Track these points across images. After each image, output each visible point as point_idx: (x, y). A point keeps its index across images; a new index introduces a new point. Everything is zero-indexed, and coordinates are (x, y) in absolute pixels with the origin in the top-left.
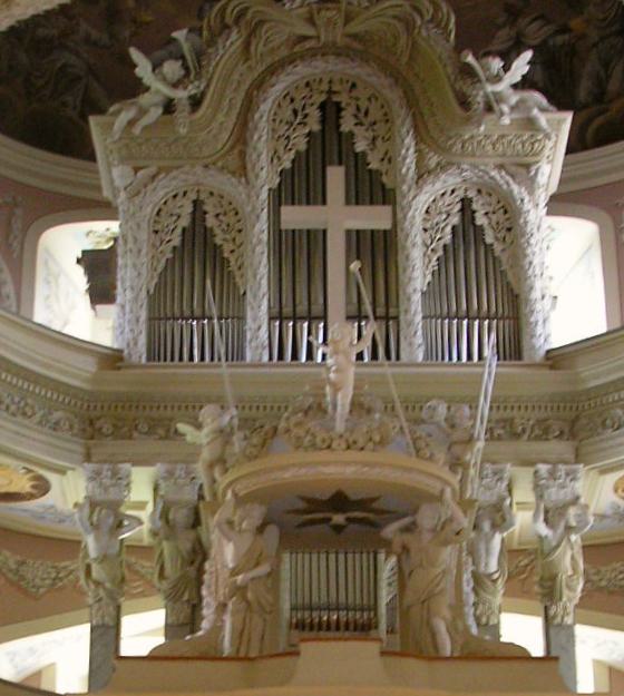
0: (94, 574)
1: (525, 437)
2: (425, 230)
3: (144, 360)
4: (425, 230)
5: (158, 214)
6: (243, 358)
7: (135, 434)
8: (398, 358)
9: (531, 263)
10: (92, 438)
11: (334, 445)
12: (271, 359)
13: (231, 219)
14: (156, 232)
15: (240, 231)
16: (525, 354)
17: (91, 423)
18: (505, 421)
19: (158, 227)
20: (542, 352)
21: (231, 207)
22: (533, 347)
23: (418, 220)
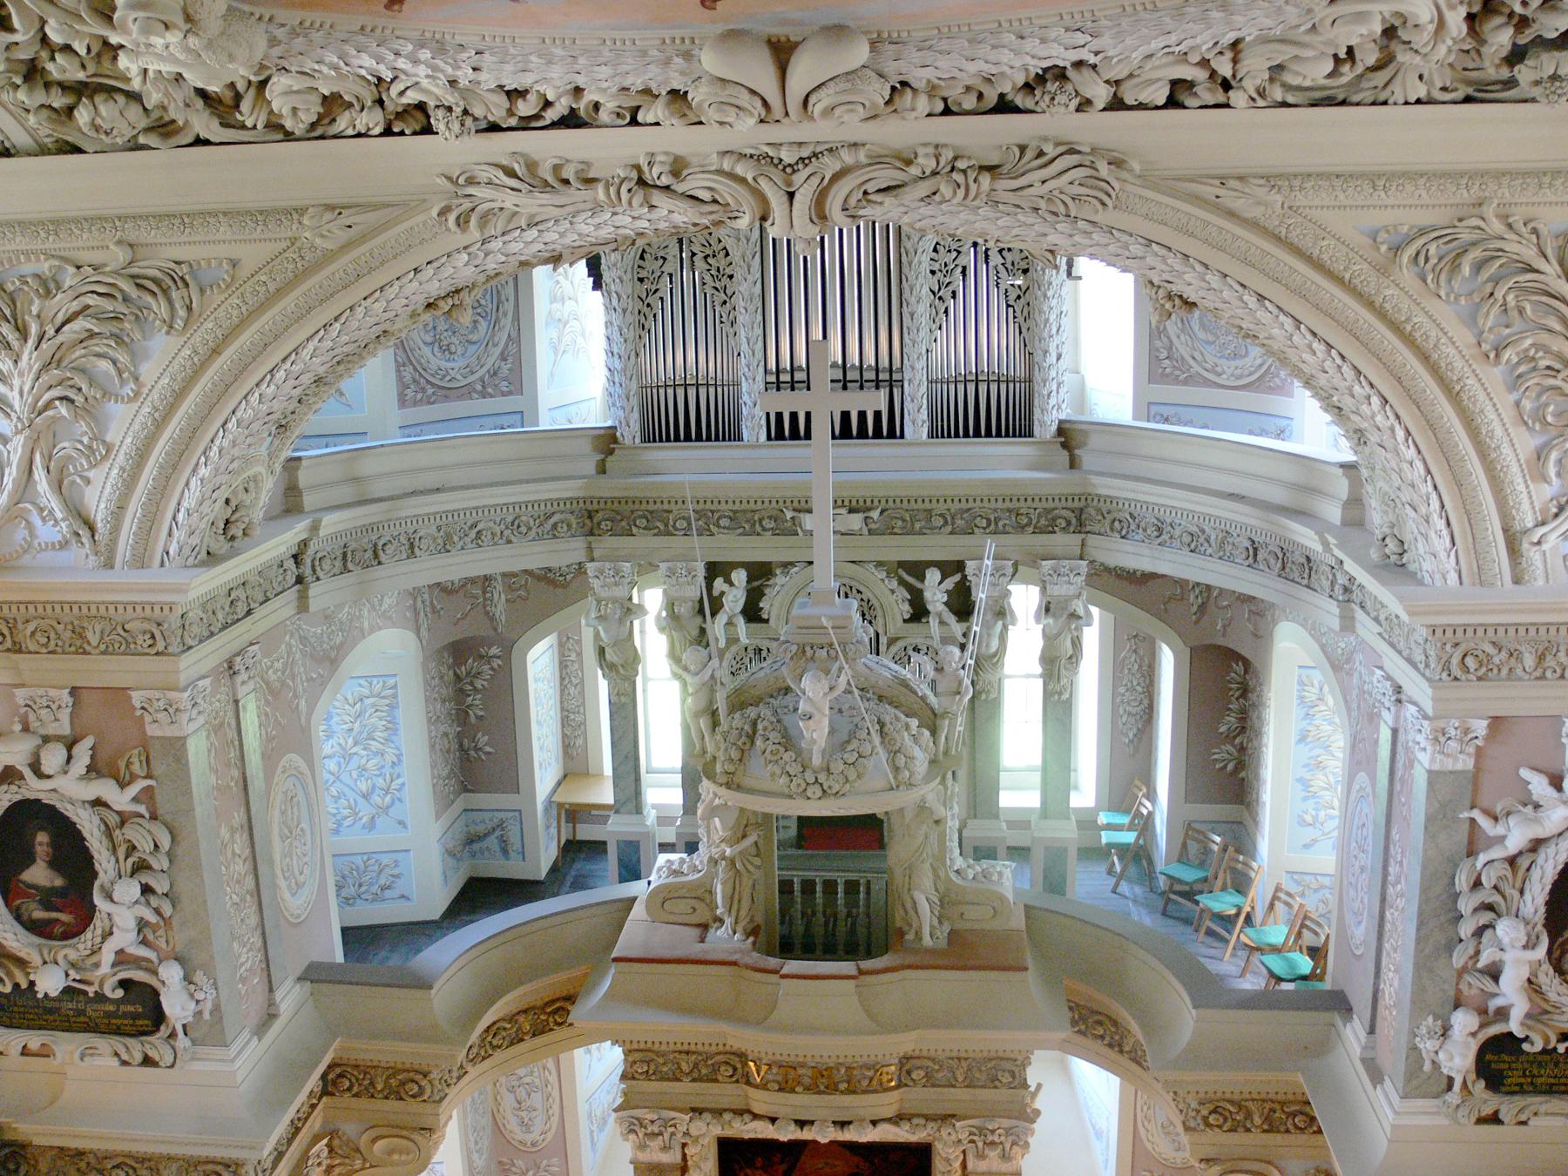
0: (607, 656)
1: (1031, 529)
2: (933, 272)
3: (638, 440)
4: (933, 272)
5: (642, 258)
6: (740, 439)
7: (635, 530)
8: (902, 436)
9: (1047, 320)
10: (591, 533)
11: (809, 793)
12: (769, 438)
13: (723, 263)
14: (641, 280)
15: (731, 277)
16: (1037, 430)
17: (590, 517)
18: (1009, 511)
19: (643, 274)
20: (1054, 428)
21: (721, 246)
22: (1043, 423)
23: (925, 259)
